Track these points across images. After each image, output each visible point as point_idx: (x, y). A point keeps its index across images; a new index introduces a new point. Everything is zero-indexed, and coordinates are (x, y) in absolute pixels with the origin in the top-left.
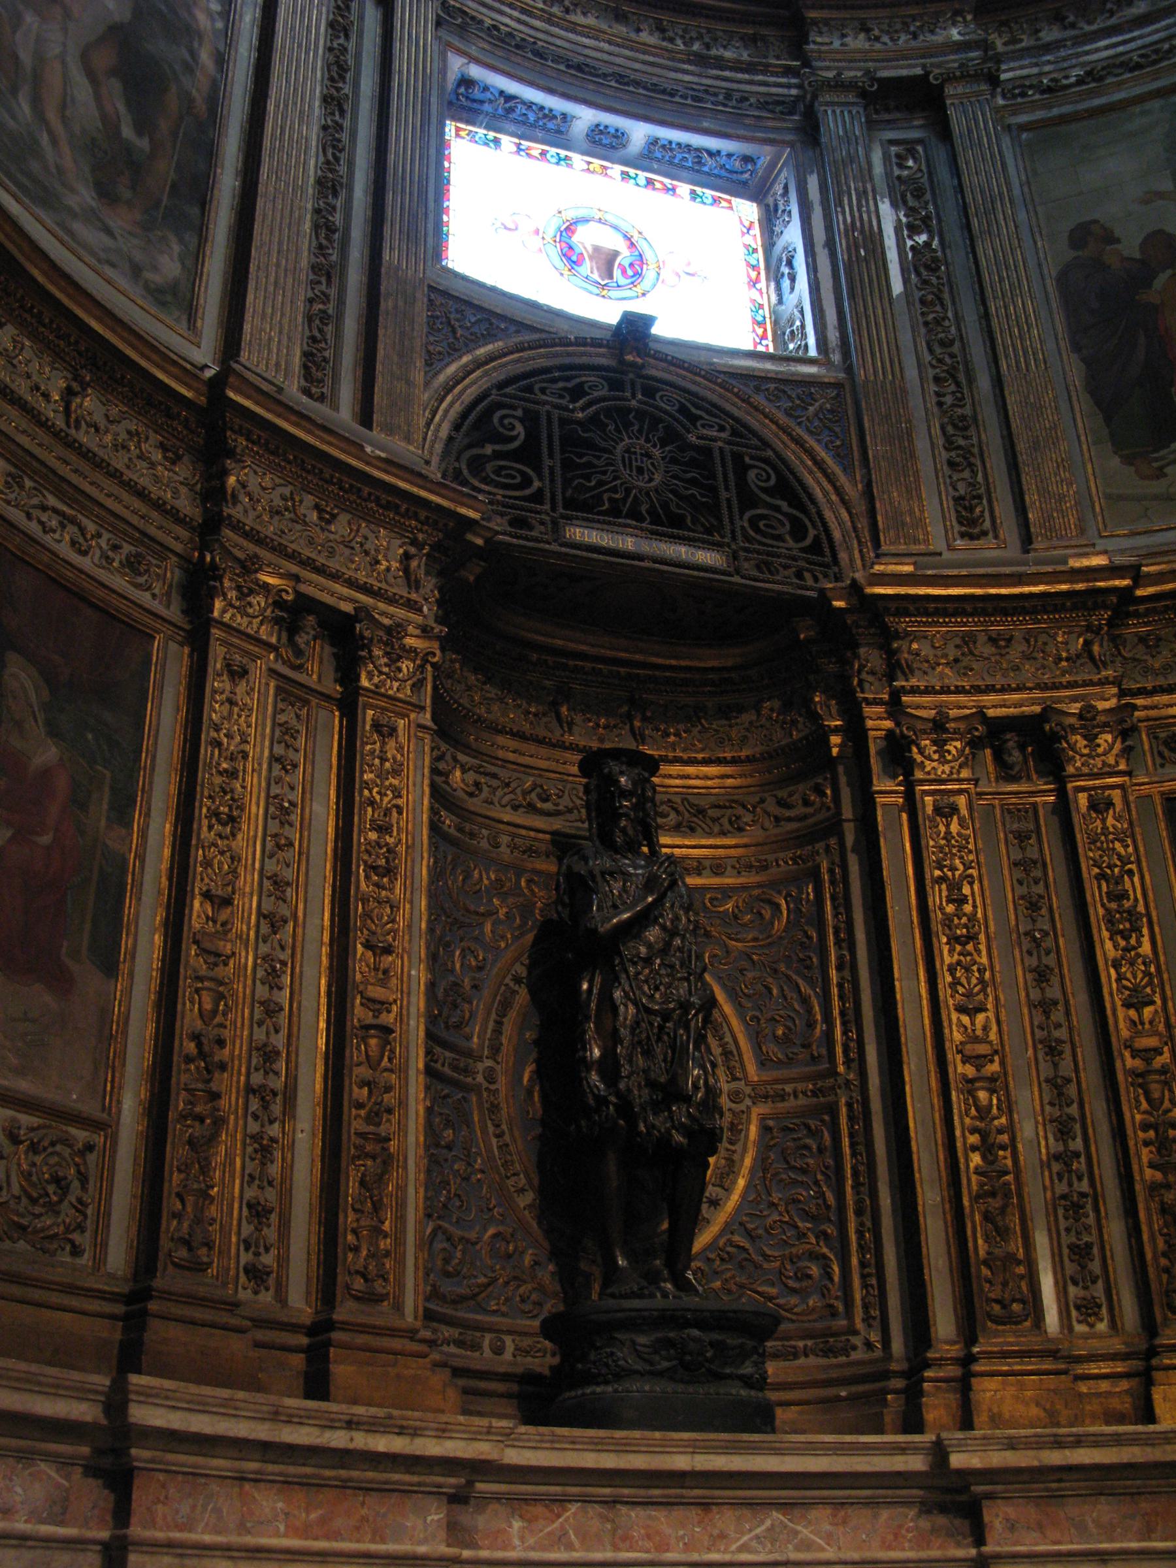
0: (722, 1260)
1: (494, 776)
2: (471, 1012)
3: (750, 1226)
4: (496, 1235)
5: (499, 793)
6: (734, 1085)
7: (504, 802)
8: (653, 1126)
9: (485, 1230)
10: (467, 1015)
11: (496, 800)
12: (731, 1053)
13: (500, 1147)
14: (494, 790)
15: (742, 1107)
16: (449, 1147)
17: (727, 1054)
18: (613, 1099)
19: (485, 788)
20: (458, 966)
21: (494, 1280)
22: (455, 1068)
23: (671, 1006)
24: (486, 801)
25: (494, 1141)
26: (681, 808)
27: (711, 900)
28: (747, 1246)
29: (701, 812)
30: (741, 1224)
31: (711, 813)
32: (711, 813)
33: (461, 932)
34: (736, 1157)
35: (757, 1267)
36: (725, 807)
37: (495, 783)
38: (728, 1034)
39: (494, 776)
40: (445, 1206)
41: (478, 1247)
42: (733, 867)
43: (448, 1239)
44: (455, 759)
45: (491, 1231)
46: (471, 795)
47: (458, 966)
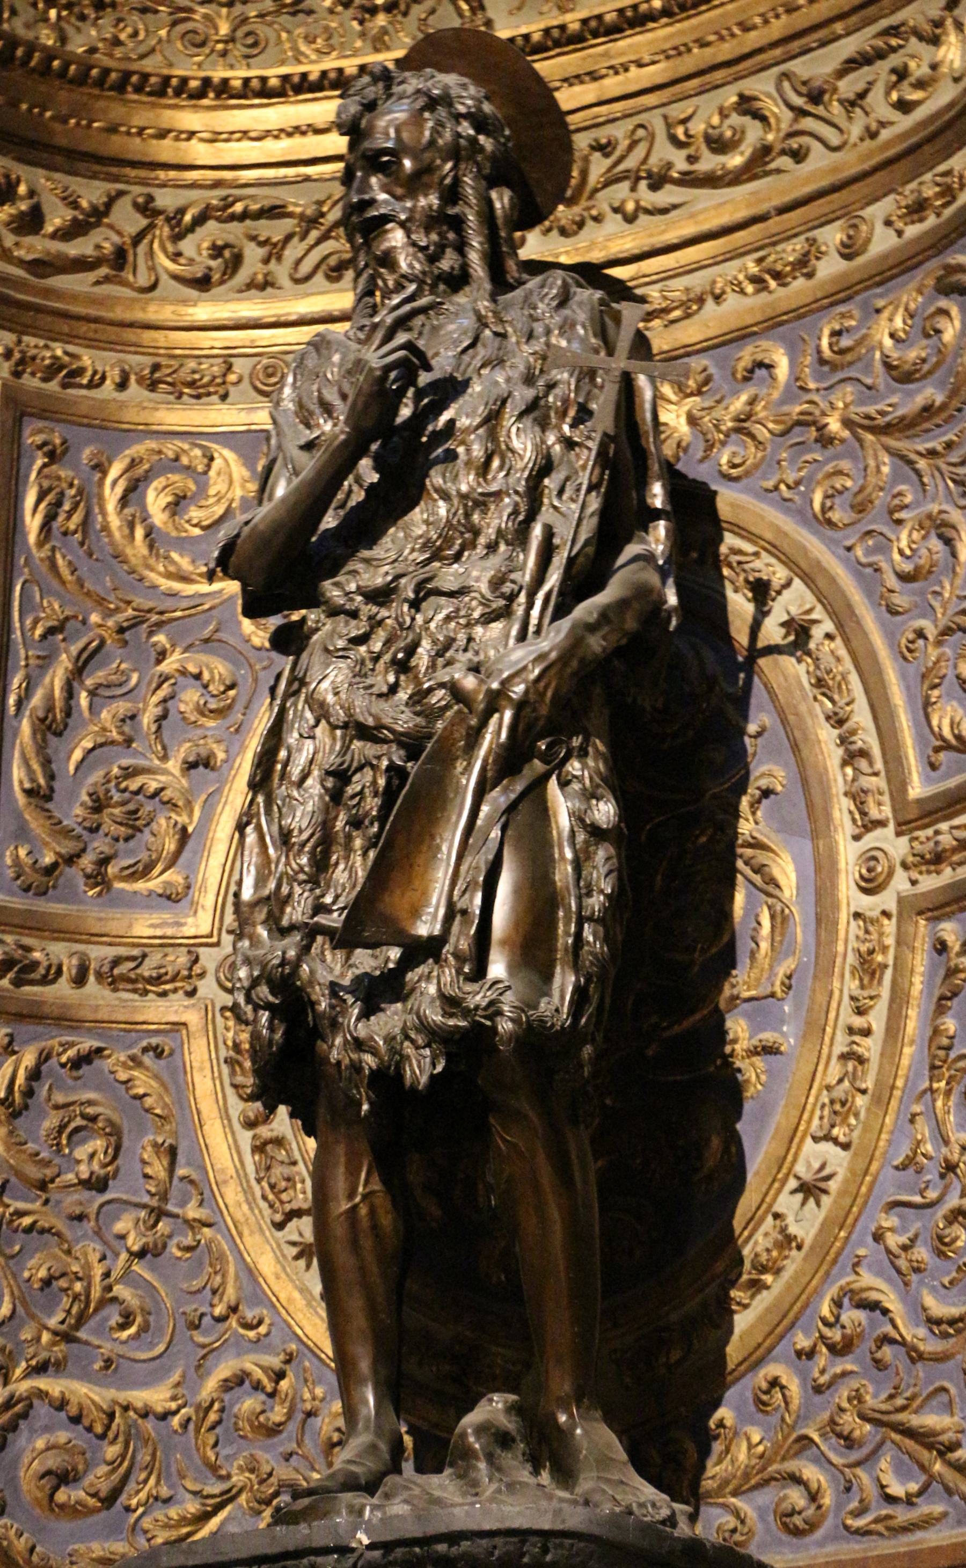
0: (833, 1349)
1: (274, 212)
2: (184, 836)
3: (893, 1240)
4: (239, 1380)
5: (293, 251)
6: (870, 840)
7: (306, 268)
8: (359, 1044)
9: (201, 1368)
10: (170, 845)
11: (281, 271)
12: (864, 753)
13: (259, 1148)
14: (275, 251)
15: (887, 900)
16: (98, 1184)
17: (853, 756)
18: (263, 991)
19: (253, 254)
20: (147, 720)
21: (228, 1498)
22: (114, 982)
23: (439, 697)
24: (250, 285)
25: (246, 1138)
26: (772, 107)
27: (836, 334)
28: (892, 1301)
29: (816, 97)
30: (878, 1237)
31: (848, 86)
32: (848, 86)
33: (161, 638)
34: (871, 1047)
35: (915, 1356)
36: (881, 55)
37: (275, 230)
38: (862, 704)
39: (274, 212)
40: (66, 1337)
41: (176, 1421)
42: (888, 223)
43: (76, 1420)
44: (147, 208)
45: (224, 1370)
46: (203, 283)
47: (147, 720)
